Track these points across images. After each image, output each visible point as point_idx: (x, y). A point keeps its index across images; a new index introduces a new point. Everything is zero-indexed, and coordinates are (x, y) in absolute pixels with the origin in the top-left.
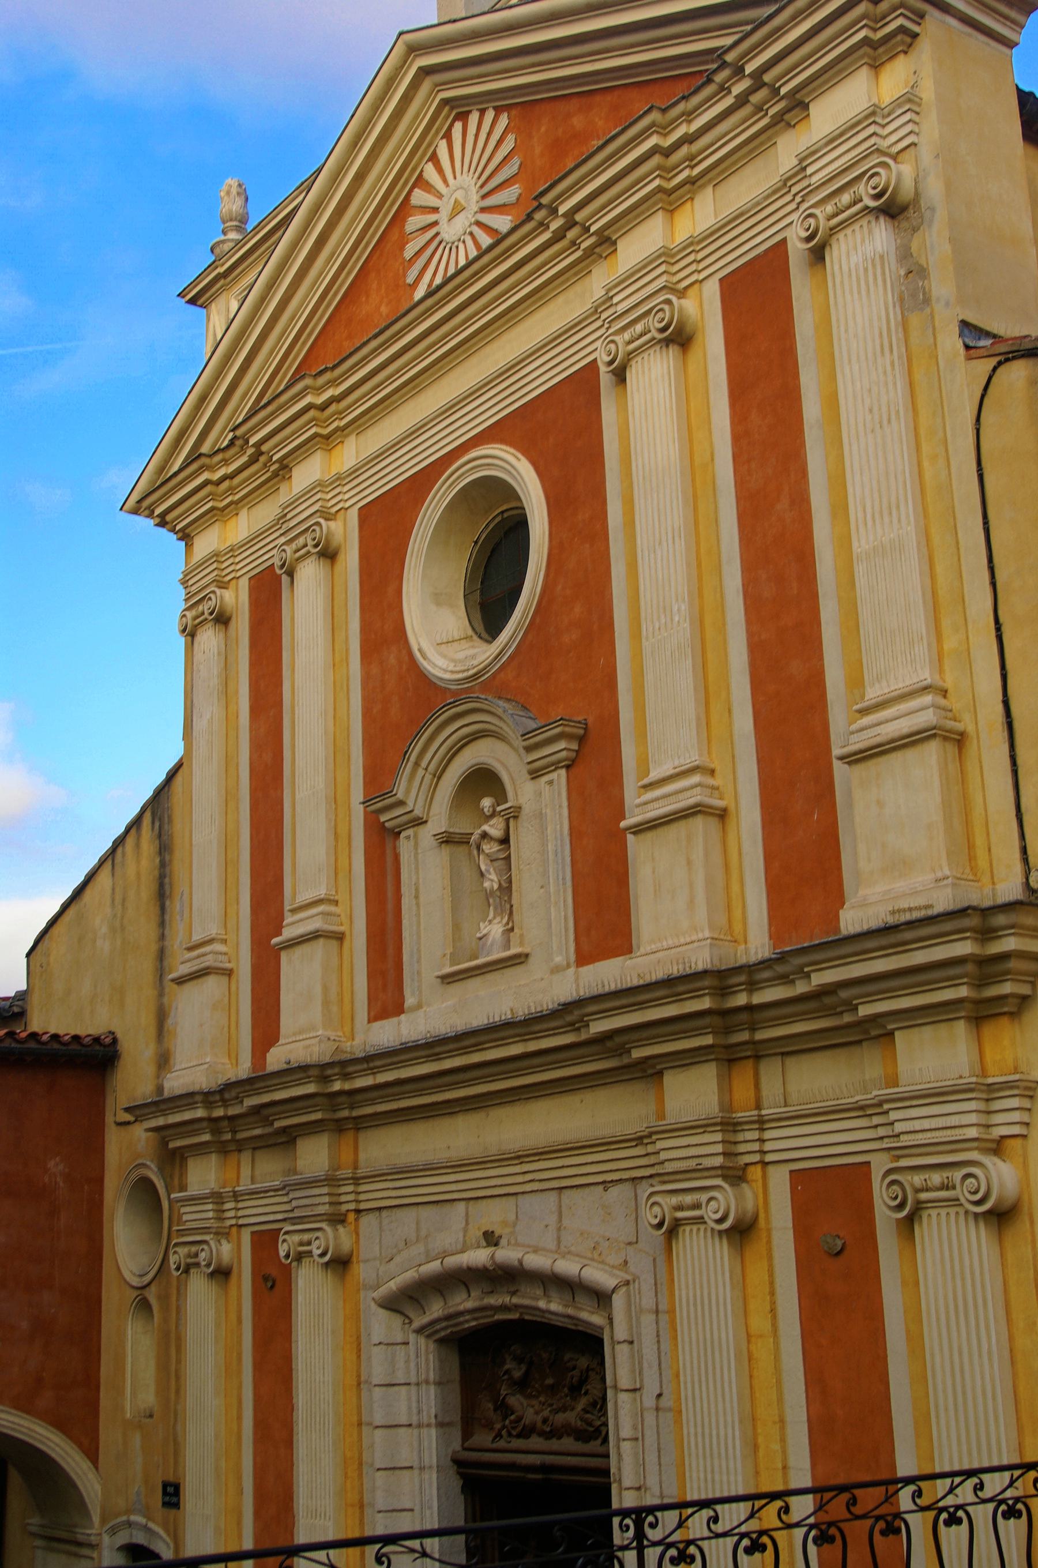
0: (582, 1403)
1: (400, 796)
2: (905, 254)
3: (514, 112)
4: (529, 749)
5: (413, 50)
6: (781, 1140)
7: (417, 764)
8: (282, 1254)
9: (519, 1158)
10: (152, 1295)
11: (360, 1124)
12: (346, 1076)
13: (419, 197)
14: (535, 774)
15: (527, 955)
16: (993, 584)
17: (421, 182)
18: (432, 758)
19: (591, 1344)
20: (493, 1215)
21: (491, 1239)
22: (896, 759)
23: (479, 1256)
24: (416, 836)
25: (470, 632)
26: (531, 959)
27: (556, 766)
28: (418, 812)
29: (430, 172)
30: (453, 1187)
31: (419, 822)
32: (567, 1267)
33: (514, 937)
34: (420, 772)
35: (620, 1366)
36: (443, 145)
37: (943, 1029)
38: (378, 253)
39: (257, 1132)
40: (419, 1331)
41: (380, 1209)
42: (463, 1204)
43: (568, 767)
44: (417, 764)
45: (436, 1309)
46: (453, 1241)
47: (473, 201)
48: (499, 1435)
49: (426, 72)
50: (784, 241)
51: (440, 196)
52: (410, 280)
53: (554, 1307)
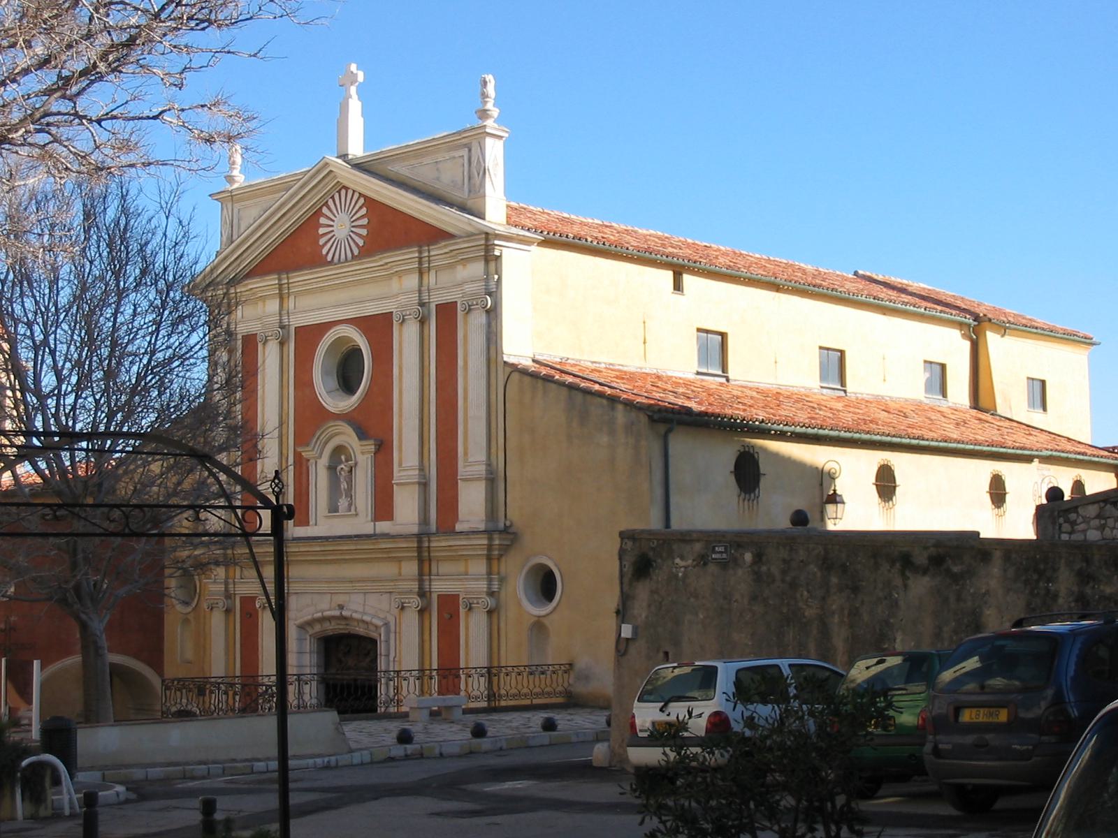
0: (368, 659)
2: (489, 325)
7: (318, 438)
8: (257, 606)
10: (191, 617)
13: (325, 210)
14: (363, 453)
17: (326, 204)
19: (374, 642)
21: (341, 607)
23: (337, 613)
24: (316, 462)
25: (338, 387)
29: (330, 202)
33: (353, 508)
35: (382, 648)
36: (337, 194)
44: (318, 438)
45: (318, 628)
46: (324, 606)
47: (348, 224)
48: (338, 670)
50: (456, 302)
51: (333, 221)
52: (321, 243)
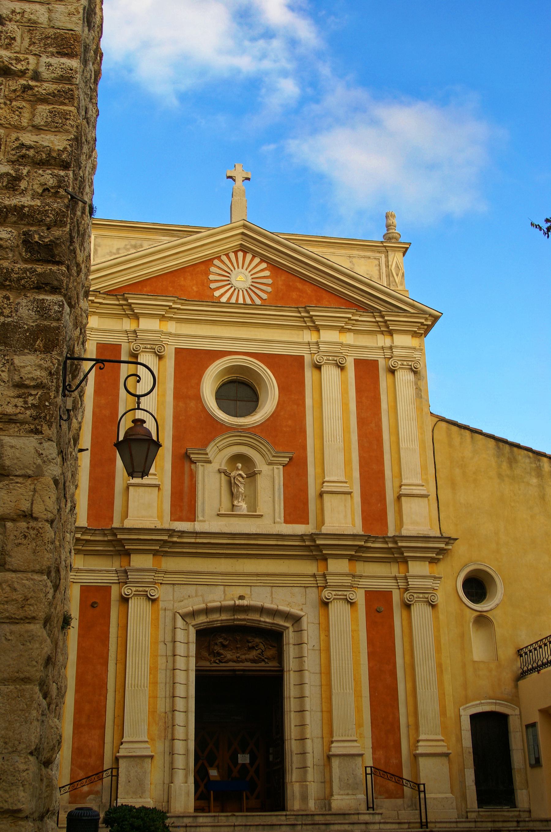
1: (208, 452)
3: (269, 265)
4: (274, 456)
5: (245, 226)
6: (364, 582)
9: (258, 575)
11: (166, 554)
12: (179, 537)
15: (262, 516)
16: (435, 468)
18: (221, 444)
20: (240, 591)
22: (416, 499)
26: (263, 517)
27: (280, 464)
28: (211, 459)
30: (220, 581)
31: (210, 462)
32: (283, 608)
34: (216, 447)
37: (422, 563)
38: (192, 268)
39: (101, 548)
40: (193, 626)
41: (173, 584)
42: (222, 587)
43: (283, 466)
45: (202, 619)
49: (243, 234)
53: (268, 620)
